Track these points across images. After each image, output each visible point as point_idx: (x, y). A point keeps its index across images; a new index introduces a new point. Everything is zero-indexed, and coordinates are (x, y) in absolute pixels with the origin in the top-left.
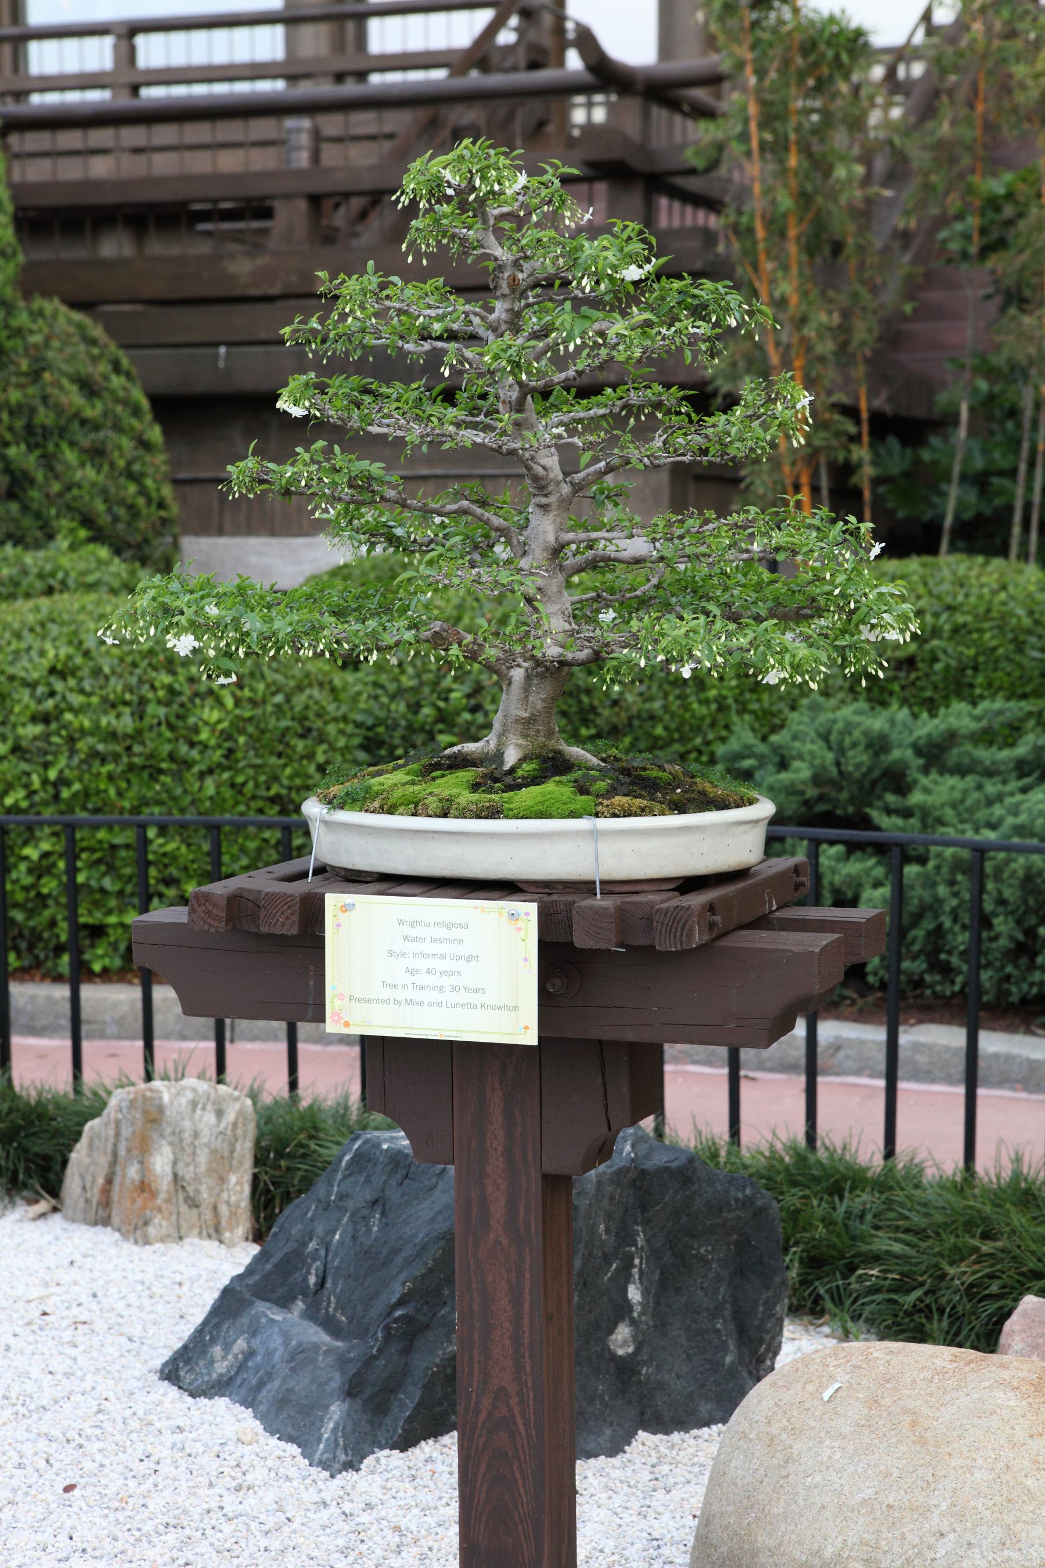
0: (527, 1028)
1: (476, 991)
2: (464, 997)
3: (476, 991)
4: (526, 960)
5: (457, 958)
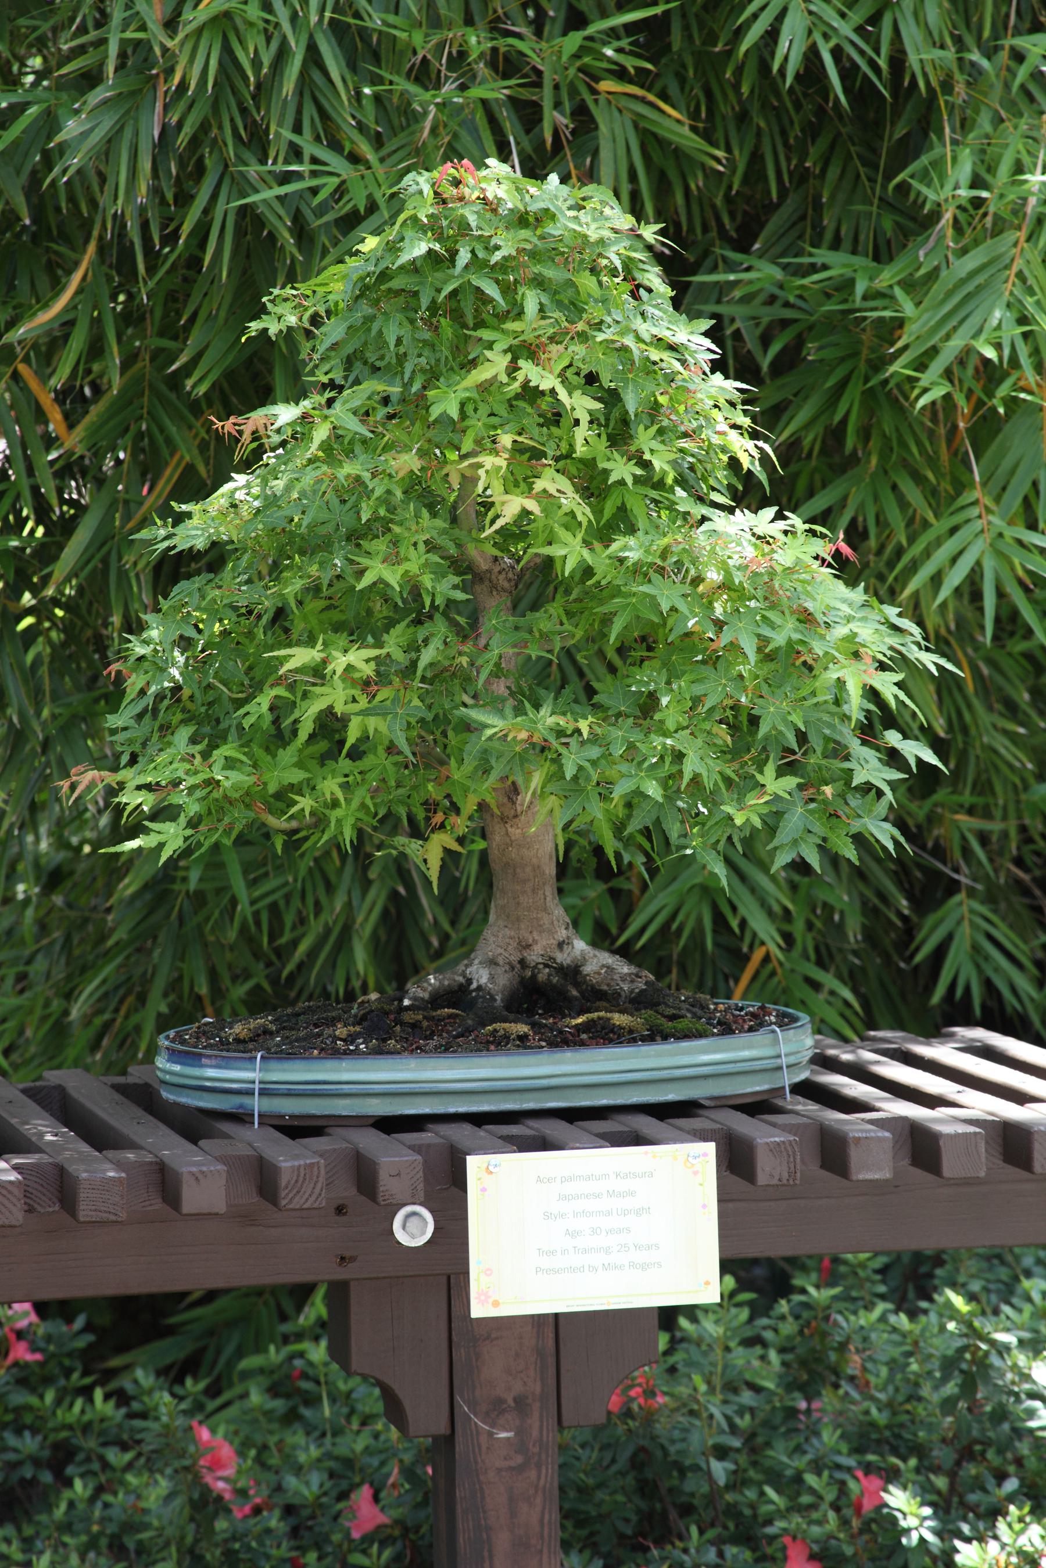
0: (707, 1283)
1: (649, 1247)
3: (649, 1247)
4: (704, 1206)
5: (626, 1213)
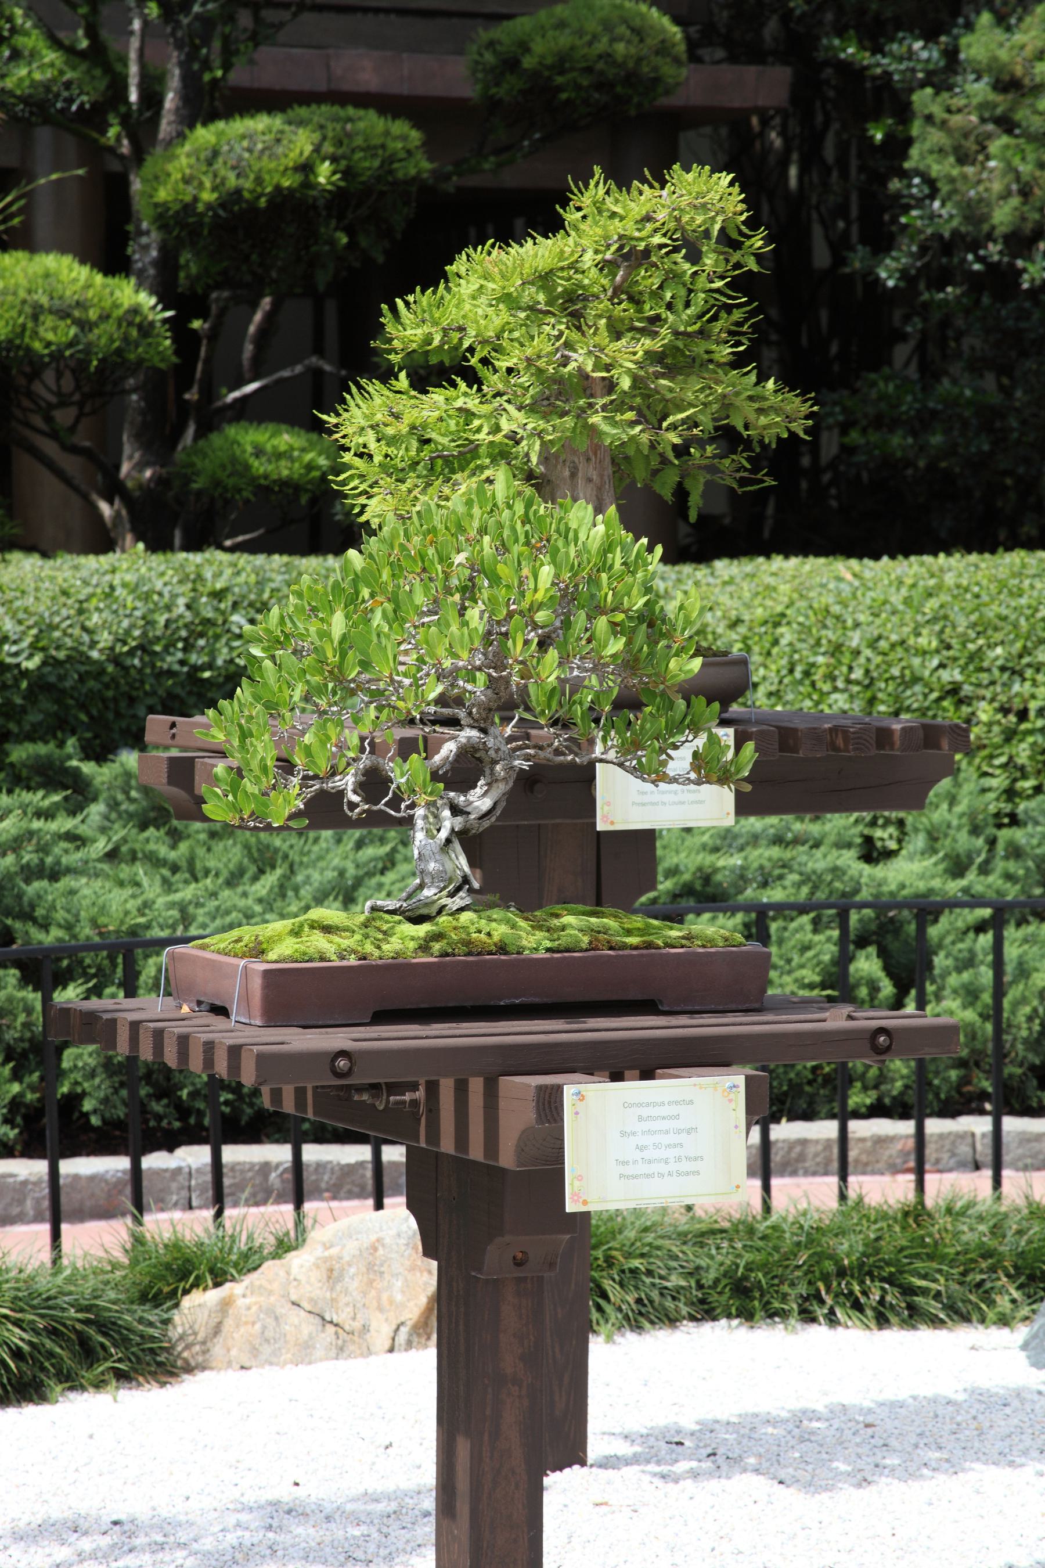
1: (696, 1159)
2: (685, 1166)
3: (696, 1159)
4: (736, 1127)
5: (679, 1132)
